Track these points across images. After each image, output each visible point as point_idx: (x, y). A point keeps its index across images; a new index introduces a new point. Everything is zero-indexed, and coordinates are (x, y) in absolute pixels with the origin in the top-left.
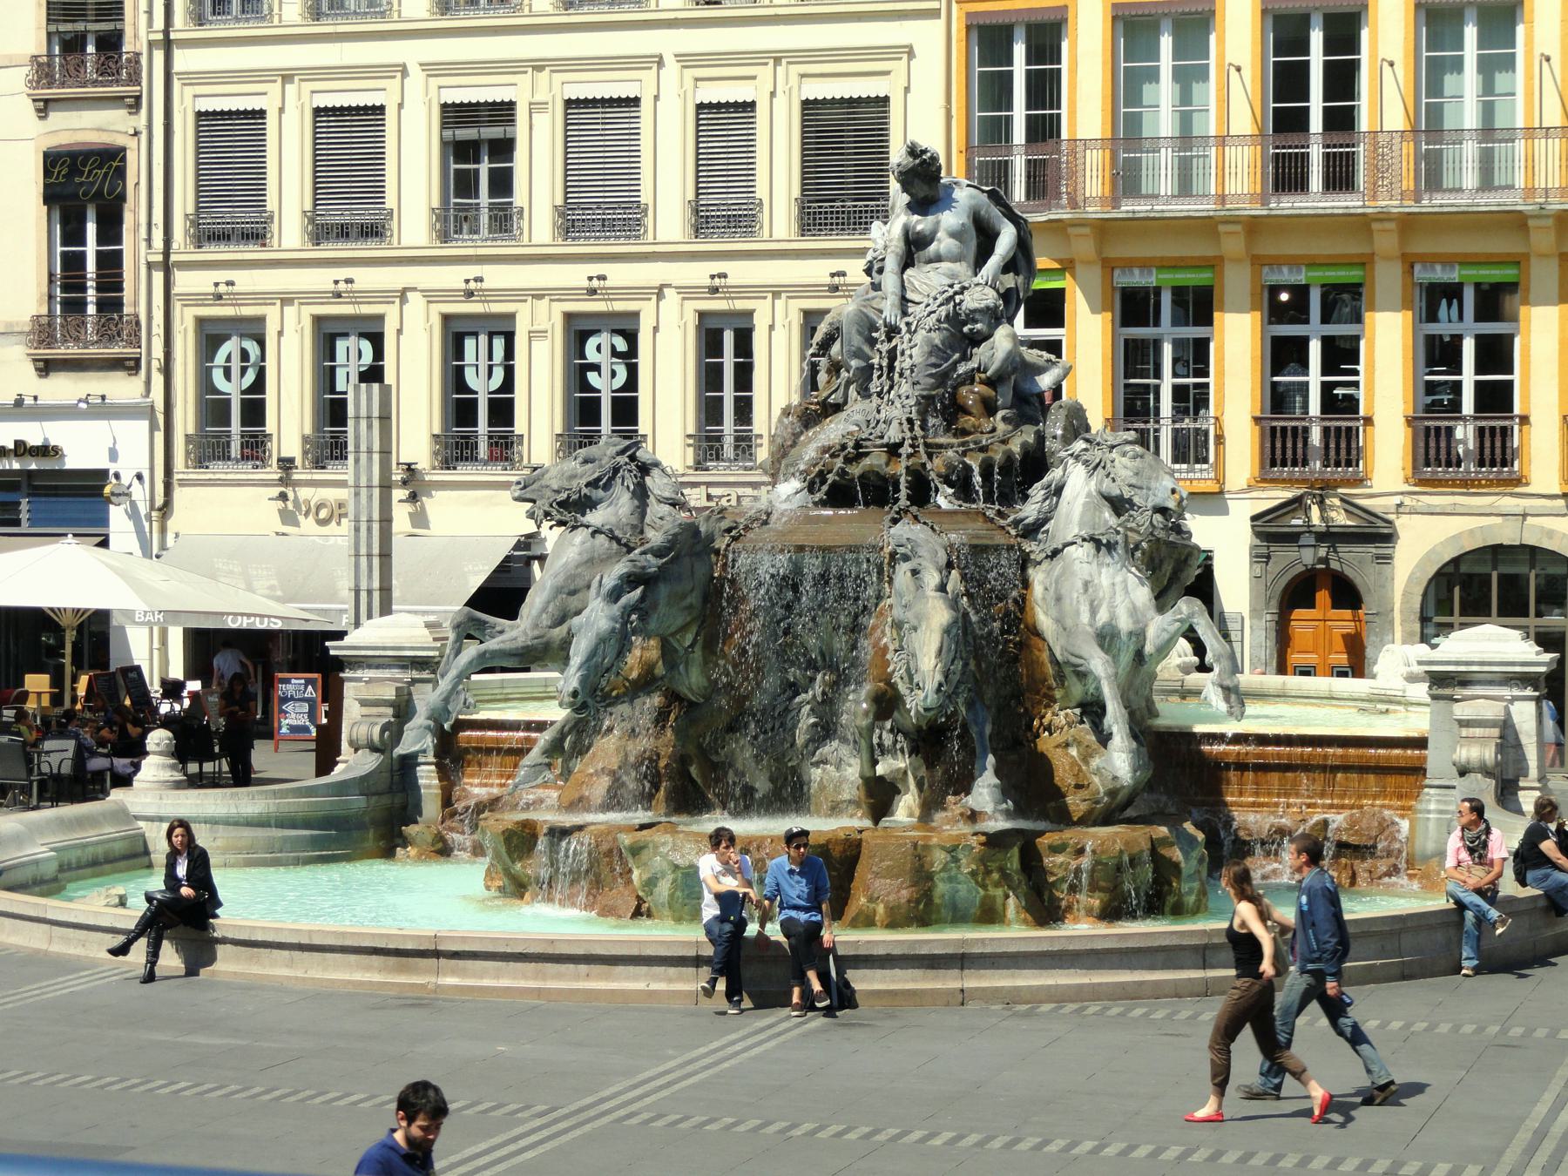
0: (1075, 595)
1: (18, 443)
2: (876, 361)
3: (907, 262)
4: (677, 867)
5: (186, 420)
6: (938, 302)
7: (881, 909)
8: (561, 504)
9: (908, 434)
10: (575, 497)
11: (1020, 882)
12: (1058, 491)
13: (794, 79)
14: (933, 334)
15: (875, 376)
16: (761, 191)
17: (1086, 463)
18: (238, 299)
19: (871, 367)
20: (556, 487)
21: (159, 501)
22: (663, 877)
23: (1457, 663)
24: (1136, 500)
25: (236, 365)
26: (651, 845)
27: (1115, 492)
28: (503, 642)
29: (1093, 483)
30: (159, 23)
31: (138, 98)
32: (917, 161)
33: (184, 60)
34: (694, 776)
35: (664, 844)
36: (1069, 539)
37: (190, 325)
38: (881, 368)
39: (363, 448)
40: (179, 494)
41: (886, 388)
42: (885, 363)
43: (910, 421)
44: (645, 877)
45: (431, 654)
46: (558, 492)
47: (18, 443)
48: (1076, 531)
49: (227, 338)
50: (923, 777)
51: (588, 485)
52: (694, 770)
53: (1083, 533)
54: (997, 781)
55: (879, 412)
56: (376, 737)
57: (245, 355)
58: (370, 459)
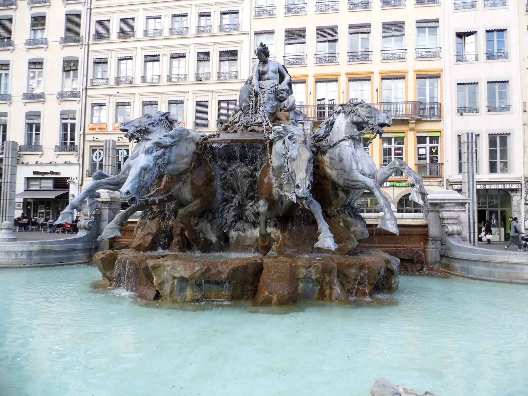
0: (349, 158)
1: (51, 171)
2: (251, 104)
3: (260, 79)
4: (174, 278)
5: (87, 167)
6: (271, 86)
7: (275, 297)
8: (137, 131)
9: (265, 120)
10: (144, 129)
11: (337, 282)
12: (332, 124)
13: (217, 96)
14: (270, 95)
15: (251, 107)
16: (209, 119)
17: (345, 112)
18: (99, 142)
19: (249, 106)
20: (136, 125)
21: (80, 184)
22: (168, 282)
23: (440, 200)
24: (370, 122)
25: (98, 156)
26: (162, 266)
27: (361, 120)
28: (108, 180)
29: (348, 120)
30: (85, 85)
31: (80, 100)
32: (264, 47)
33: (90, 92)
34: (187, 235)
35: (168, 266)
36: (341, 138)
37: (88, 147)
38: (253, 106)
39: (107, 156)
40: (84, 182)
41: (254, 112)
42: (254, 104)
43: (264, 116)
44: (159, 282)
45: (108, 200)
46: (137, 127)
47: (51, 171)
48: (344, 136)
49: (96, 150)
50: (279, 236)
51: (149, 124)
52: (186, 233)
53: (348, 136)
54: (332, 235)
55: (252, 119)
56: (86, 225)
57: (100, 154)
58: (109, 159)
